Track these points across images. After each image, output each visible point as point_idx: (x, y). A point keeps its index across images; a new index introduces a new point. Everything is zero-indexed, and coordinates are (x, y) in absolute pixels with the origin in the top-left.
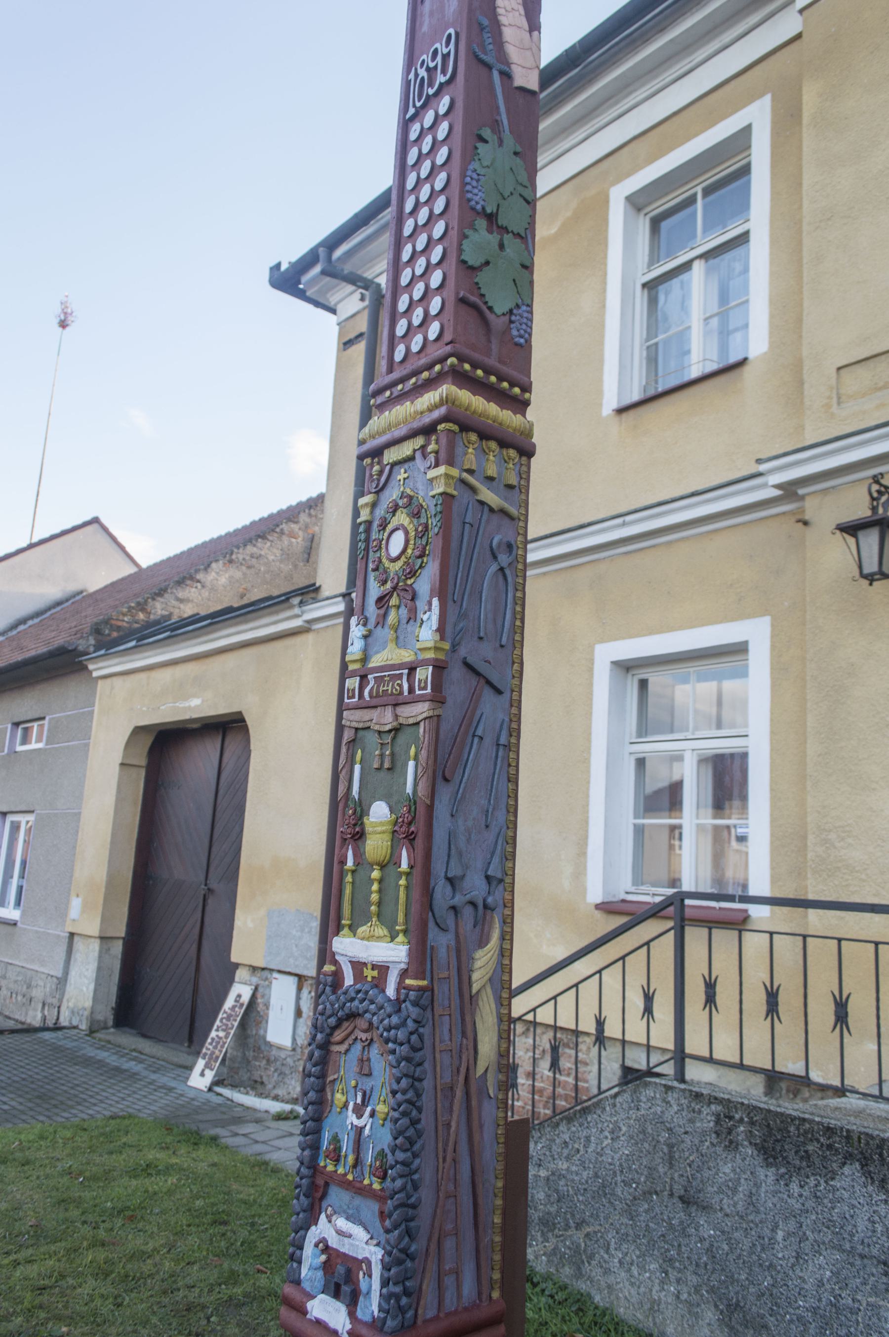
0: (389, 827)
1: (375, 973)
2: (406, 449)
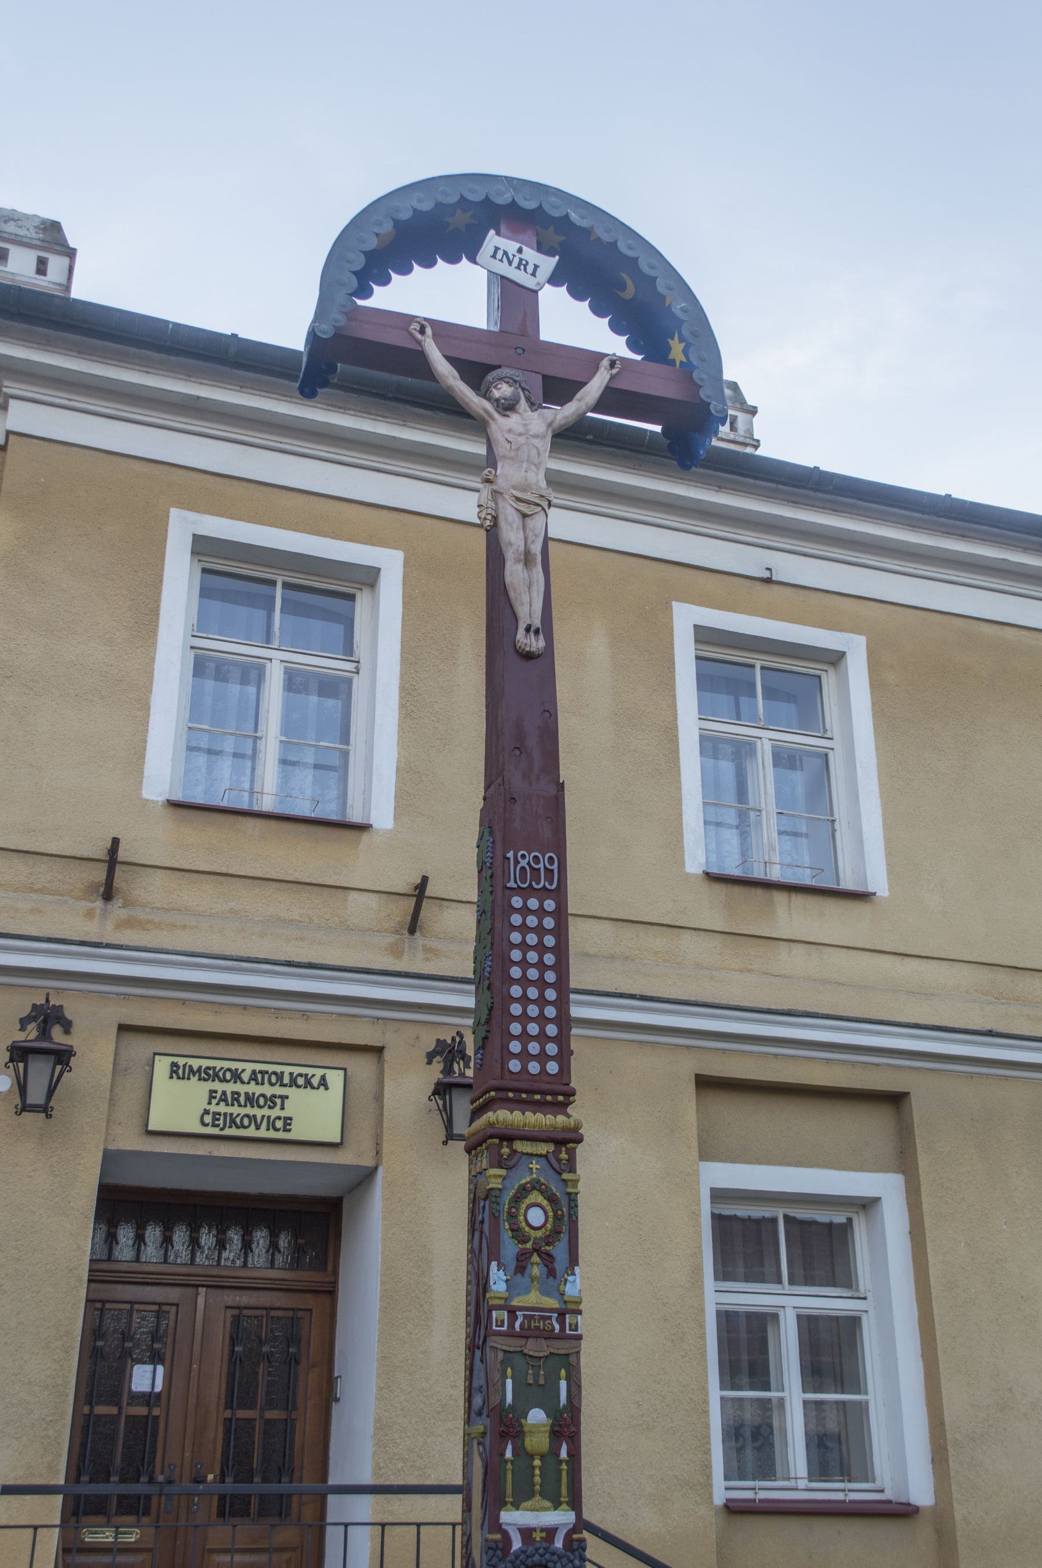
0: (548, 1428)
1: (544, 1535)
2: (543, 1148)
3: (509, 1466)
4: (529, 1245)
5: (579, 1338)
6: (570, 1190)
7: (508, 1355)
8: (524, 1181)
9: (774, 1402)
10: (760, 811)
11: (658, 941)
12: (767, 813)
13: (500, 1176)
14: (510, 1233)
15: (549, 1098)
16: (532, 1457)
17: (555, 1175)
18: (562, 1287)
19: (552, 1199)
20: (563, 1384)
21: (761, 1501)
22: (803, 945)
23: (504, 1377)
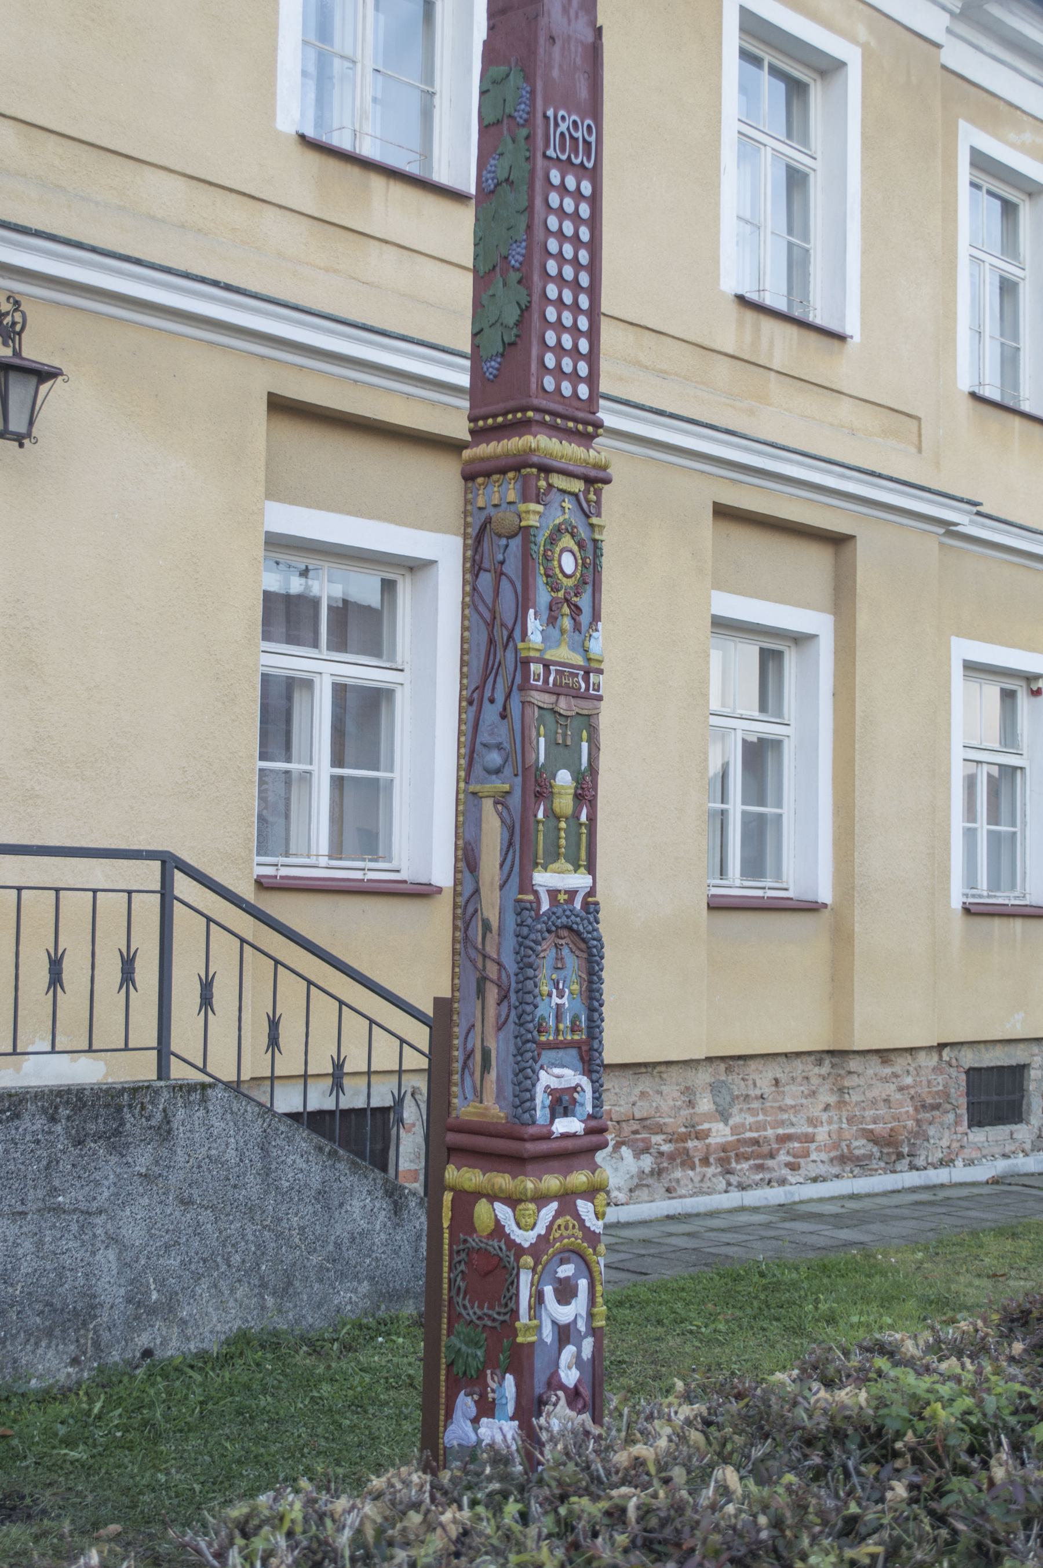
0: (573, 791)
3: (541, 827)
4: (561, 594)
5: (600, 698)
6: (597, 537)
7: (542, 711)
8: (557, 522)
9: (295, 776)
10: (354, 62)
11: (235, 214)
12: (363, 65)
13: (538, 513)
14: (544, 579)
15: (580, 427)
16: (558, 818)
17: (583, 517)
18: (587, 643)
19: (581, 545)
20: (585, 746)
21: (282, 877)
22: (395, 248)
23: (539, 735)
